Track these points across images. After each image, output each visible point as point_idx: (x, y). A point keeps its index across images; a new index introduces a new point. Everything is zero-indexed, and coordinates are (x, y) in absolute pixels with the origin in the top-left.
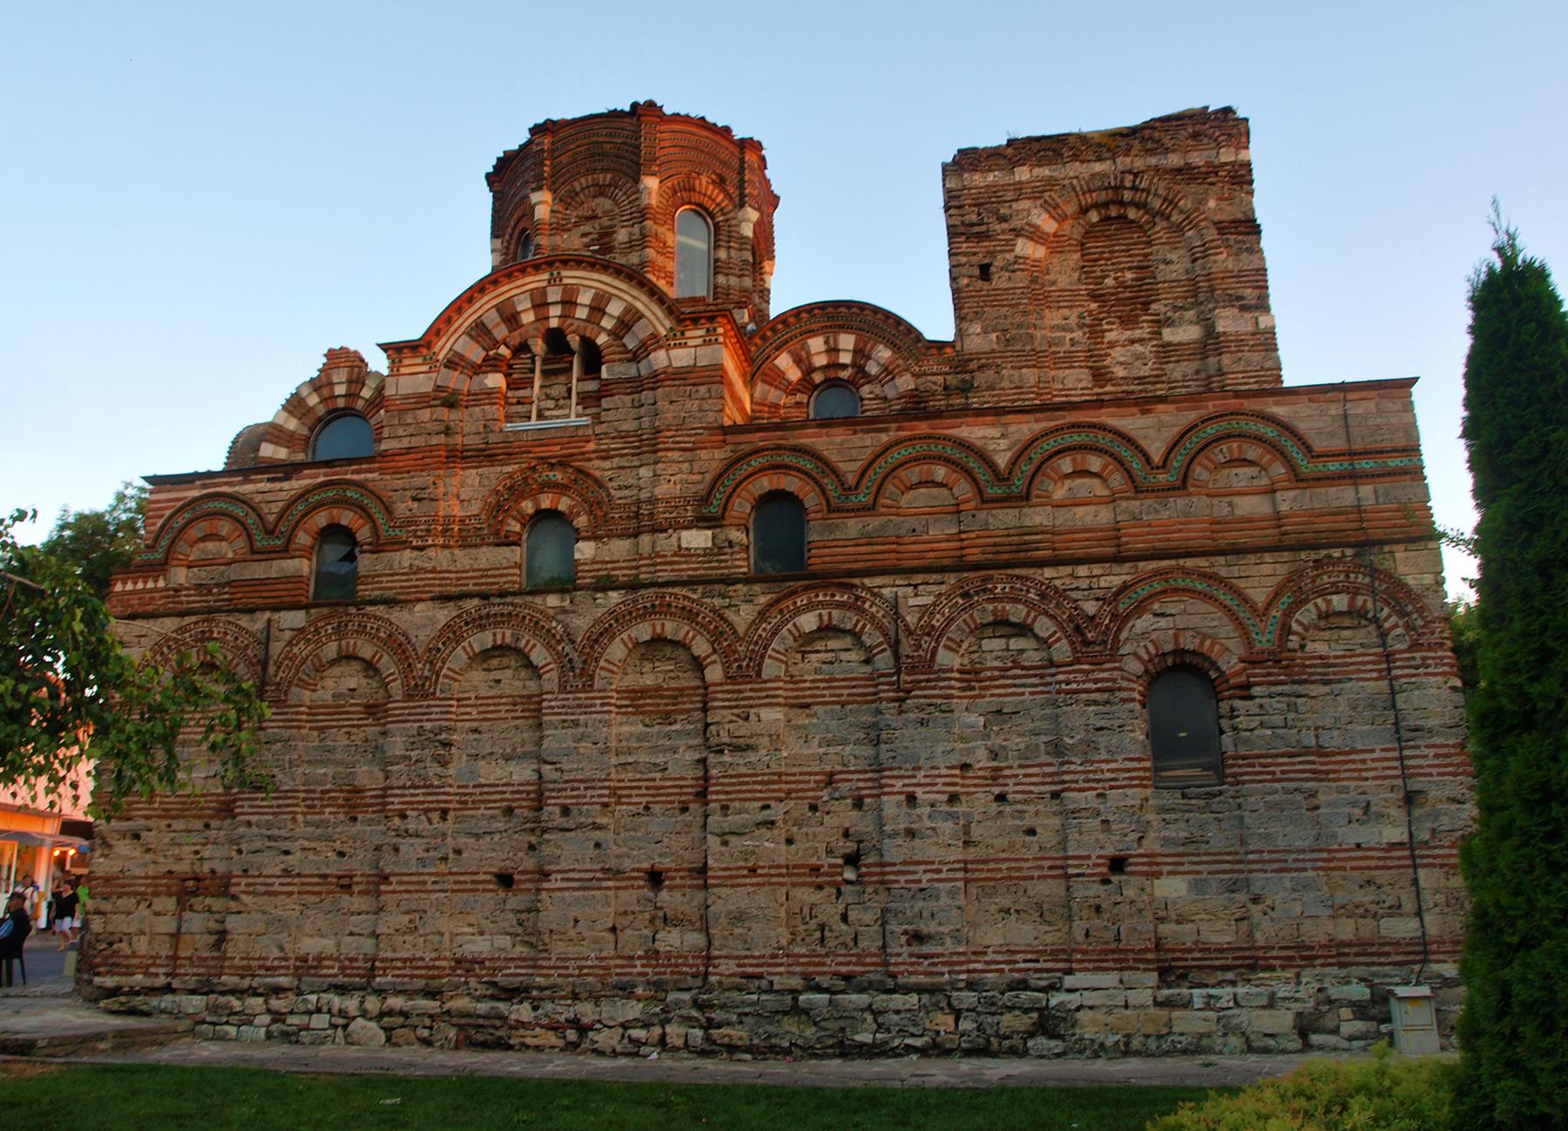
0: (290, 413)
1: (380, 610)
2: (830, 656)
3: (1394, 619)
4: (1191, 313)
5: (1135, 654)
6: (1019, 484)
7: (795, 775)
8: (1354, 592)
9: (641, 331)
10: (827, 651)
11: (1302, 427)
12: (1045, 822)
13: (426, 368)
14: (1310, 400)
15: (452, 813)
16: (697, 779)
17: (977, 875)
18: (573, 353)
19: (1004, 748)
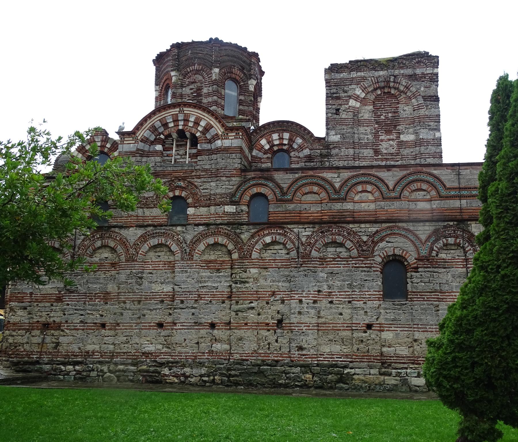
0: (79, 152)
1: (117, 230)
2: (275, 251)
3: (470, 247)
4: (411, 130)
5: (379, 255)
6: (343, 194)
7: (261, 292)
8: (457, 237)
9: (212, 132)
10: (274, 250)
11: (443, 178)
12: (346, 311)
13: (134, 142)
14: (447, 169)
16: (228, 292)
17: (322, 328)
18: (187, 138)
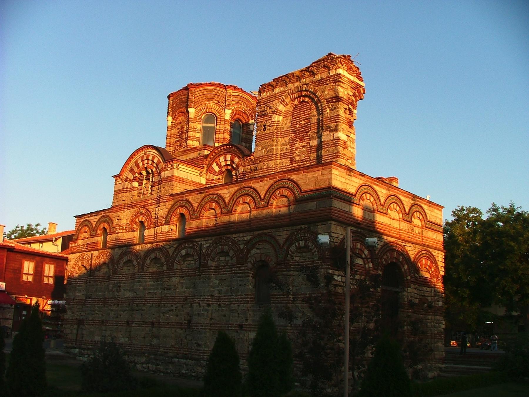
3: (315, 249)
7: (179, 297)
11: (299, 183)
15: (120, 305)
19: (221, 290)
